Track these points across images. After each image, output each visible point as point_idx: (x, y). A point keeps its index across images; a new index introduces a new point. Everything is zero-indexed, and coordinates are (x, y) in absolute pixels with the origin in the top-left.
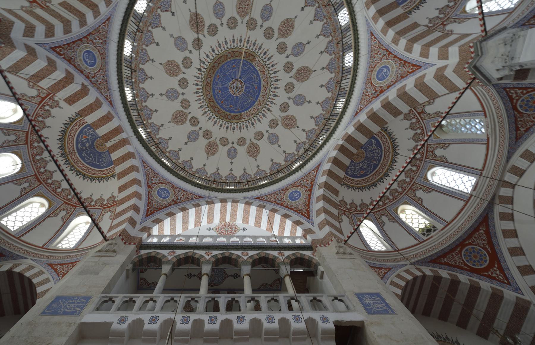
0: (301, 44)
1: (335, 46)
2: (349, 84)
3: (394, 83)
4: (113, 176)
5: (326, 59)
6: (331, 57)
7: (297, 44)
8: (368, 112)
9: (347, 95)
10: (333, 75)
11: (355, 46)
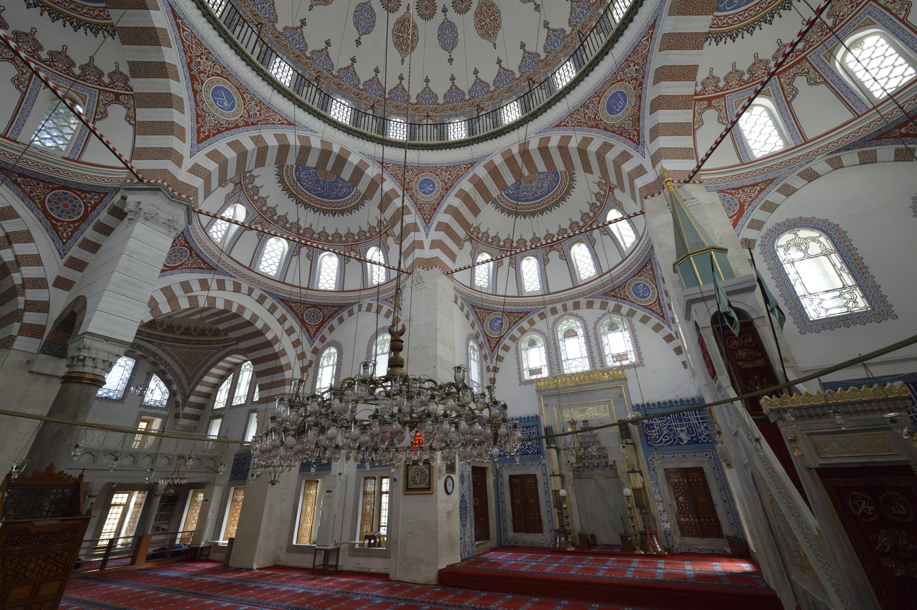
0: (367, 32)
1: (320, 68)
2: (243, 46)
3: (197, 102)
5: (314, 42)
6: (310, 49)
7: (373, 26)
8: (167, 35)
9: (225, 27)
10: (279, 27)
11: (293, 96)
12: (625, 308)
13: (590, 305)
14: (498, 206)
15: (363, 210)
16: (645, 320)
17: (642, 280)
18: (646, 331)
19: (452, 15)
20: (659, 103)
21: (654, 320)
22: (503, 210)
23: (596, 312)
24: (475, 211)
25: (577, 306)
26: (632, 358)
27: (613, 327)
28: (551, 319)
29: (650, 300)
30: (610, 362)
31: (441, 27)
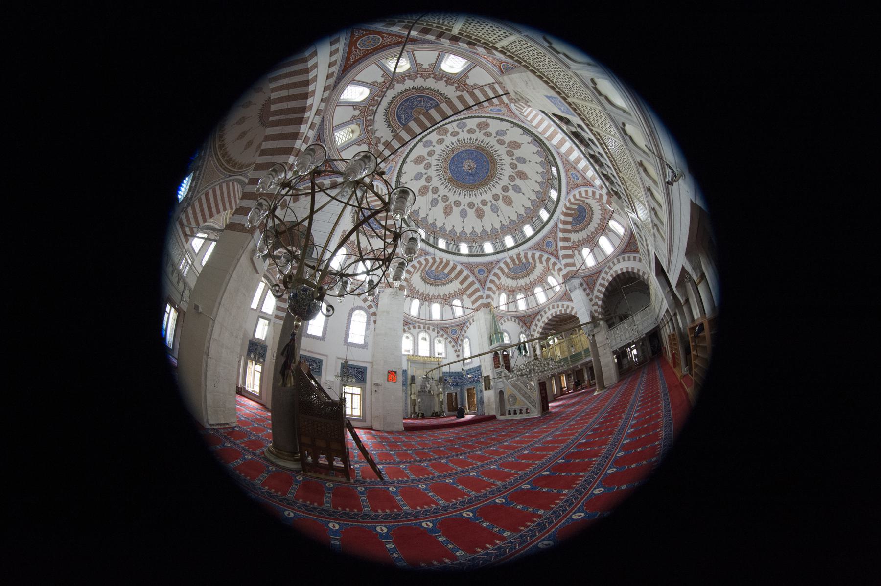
12: (445, 336)
13: (434, 330)
16: (450, 342)
17: (456, 328)
18: (450, 346)
20: (492, 282)
21: (453, 343)
23: (434, 334)
25: (429, 328)
26: (444, 355)
27: (439, 342)
28: (417, 330)
29: (455, 336)
30: (436, 355)
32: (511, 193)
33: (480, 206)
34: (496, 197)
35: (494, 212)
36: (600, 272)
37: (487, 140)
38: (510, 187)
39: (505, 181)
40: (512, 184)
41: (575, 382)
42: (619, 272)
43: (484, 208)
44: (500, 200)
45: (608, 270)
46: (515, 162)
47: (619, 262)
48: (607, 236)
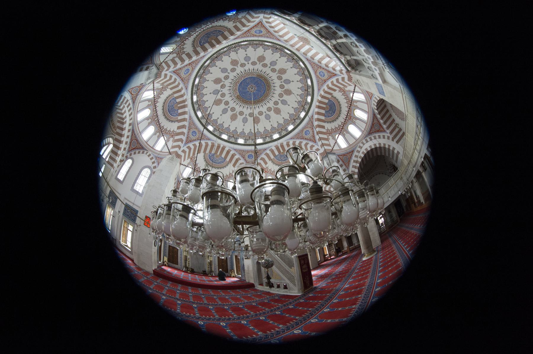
4: (333, 96)
5: (205, 84)
14: (204, 156)
15: (173, 124)
19: (229, 109)
22: (205, 158)
24: (199, 152)
31: (225, 109)
32: (280, 106)
33: (258, 115)
34: (269, 109)
35: (267, 119)
36: (353, 152)
37: (264, 70)
38: (279, 102)
39: (276, 98)
40: (281, 99)
41: (336, 250)
42: (369, 149)
43: (260, 117)
44: (272, 111)
45: (359, 149)
46: (283, 83)
47: (367, 142)
48: (354, 124)
